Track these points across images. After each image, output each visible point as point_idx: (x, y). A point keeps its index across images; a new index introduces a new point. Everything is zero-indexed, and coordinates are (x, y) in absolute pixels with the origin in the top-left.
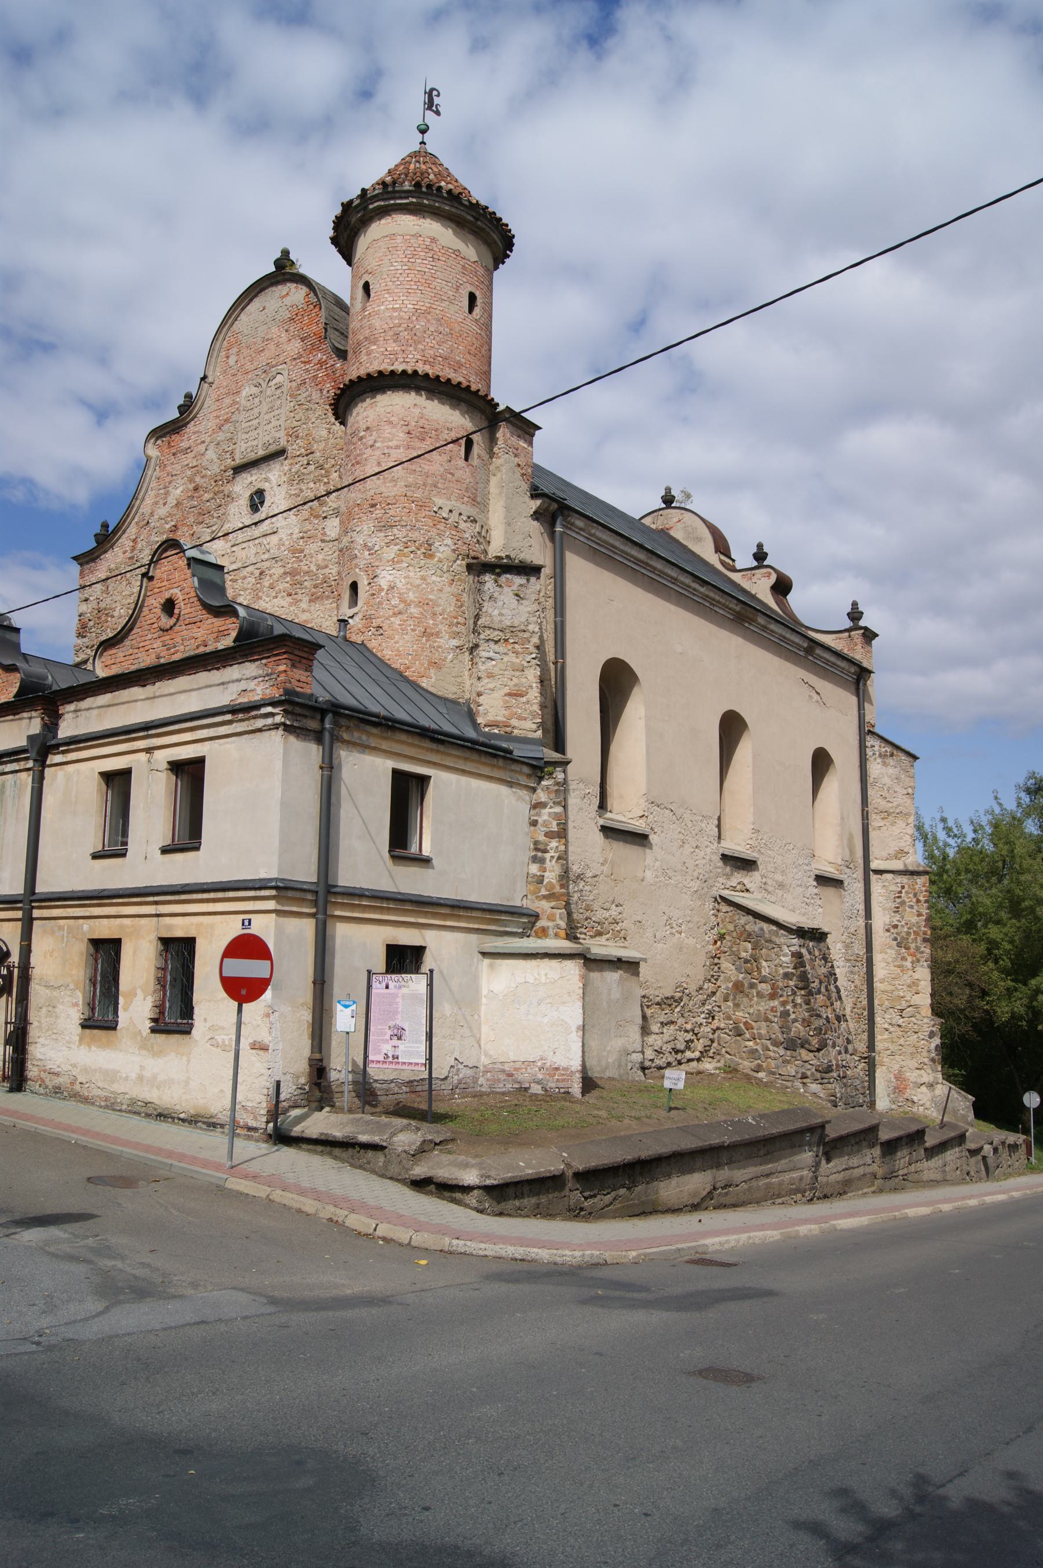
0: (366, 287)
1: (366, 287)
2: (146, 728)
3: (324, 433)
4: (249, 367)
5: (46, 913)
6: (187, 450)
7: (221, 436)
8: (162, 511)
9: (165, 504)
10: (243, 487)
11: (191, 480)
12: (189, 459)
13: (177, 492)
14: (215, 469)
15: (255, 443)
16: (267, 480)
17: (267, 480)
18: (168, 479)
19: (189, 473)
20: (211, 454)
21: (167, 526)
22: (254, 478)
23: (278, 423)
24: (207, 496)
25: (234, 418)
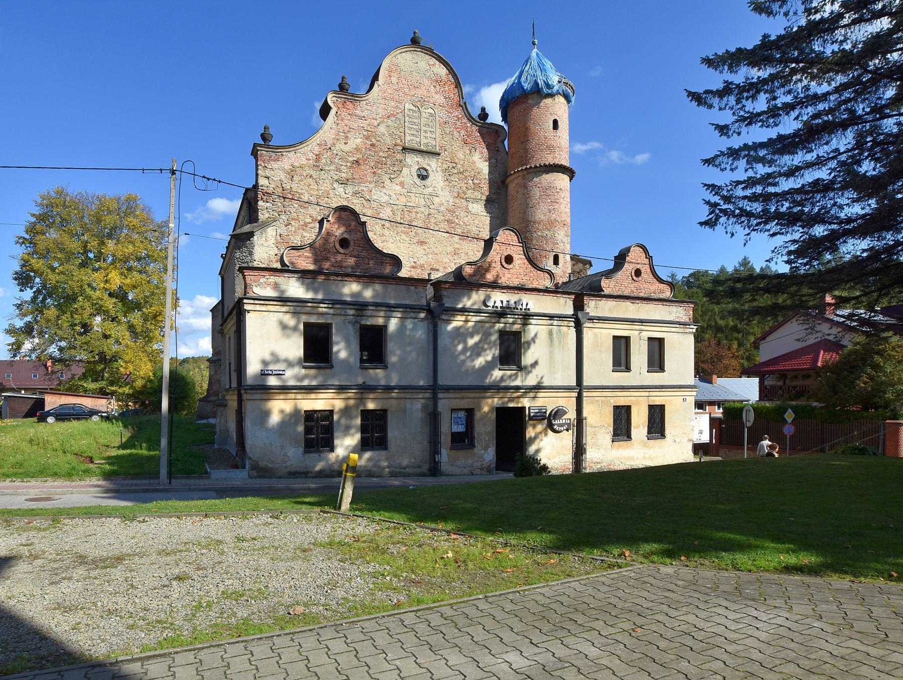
0: (555, 123)
1: (555, 123)
2: (642, 321)
3: (463, 157)
4: (407, 90)
5: (589, 394)
6: (361, 118)
7: (390, 123)
8: (346, 148)
9: (346, 143)
10: (414, 161)
11: (367, 138)
12: (364, 124)
13: (356, 141)
14: (389, 141)
15: (418, 140)
16: (429, 165)
17: (429, 165)
18: (347, 129)
19: (365, 133)
20: (382, 129)
21: (351, 159)
22: (420, 160)
23: (434, 136)
24: (381, 154)
25: (398, 116)
